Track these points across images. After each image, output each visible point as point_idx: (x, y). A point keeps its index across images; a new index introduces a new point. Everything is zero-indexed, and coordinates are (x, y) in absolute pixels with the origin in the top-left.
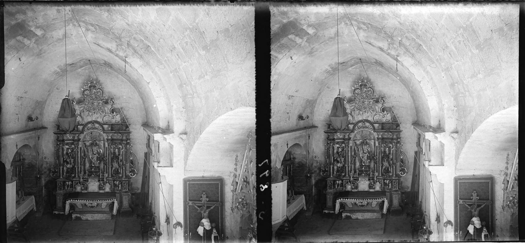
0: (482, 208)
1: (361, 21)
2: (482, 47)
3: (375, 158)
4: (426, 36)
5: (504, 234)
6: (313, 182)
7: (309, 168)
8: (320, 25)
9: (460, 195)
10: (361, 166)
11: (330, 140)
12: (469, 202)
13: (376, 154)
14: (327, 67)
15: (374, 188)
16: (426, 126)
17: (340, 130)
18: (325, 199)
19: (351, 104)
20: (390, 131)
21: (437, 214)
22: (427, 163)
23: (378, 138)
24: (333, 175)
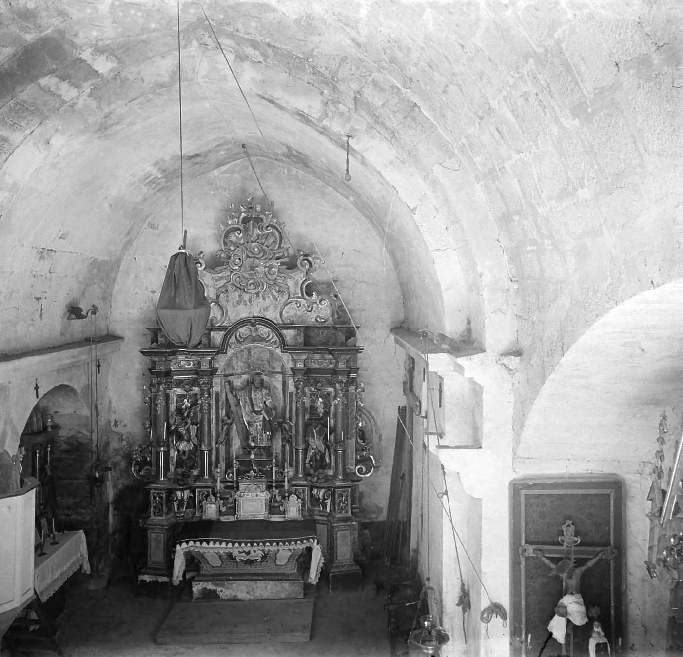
0: (589, 569)
1: (247, 36)
2: (589, 110)
3: (286, 426)
4: (432, 79)
5: (653, 642)
6: (110, 494)
7: (98, 454)
8: (128, 49)
9: (526, 531)
10: (247, 449)
11: (157, 376)
12: (554, 551)
13: (287, 416)
14: (149, 168)
15: (284, 513)
16: (430, 336)
17: (185, 347)
18: (145, 545)
19: (217, 272)
20: (327, 350)
21: (463, 585)
22: (432, 442)
23: (294, 371)
24: (165, 476)
